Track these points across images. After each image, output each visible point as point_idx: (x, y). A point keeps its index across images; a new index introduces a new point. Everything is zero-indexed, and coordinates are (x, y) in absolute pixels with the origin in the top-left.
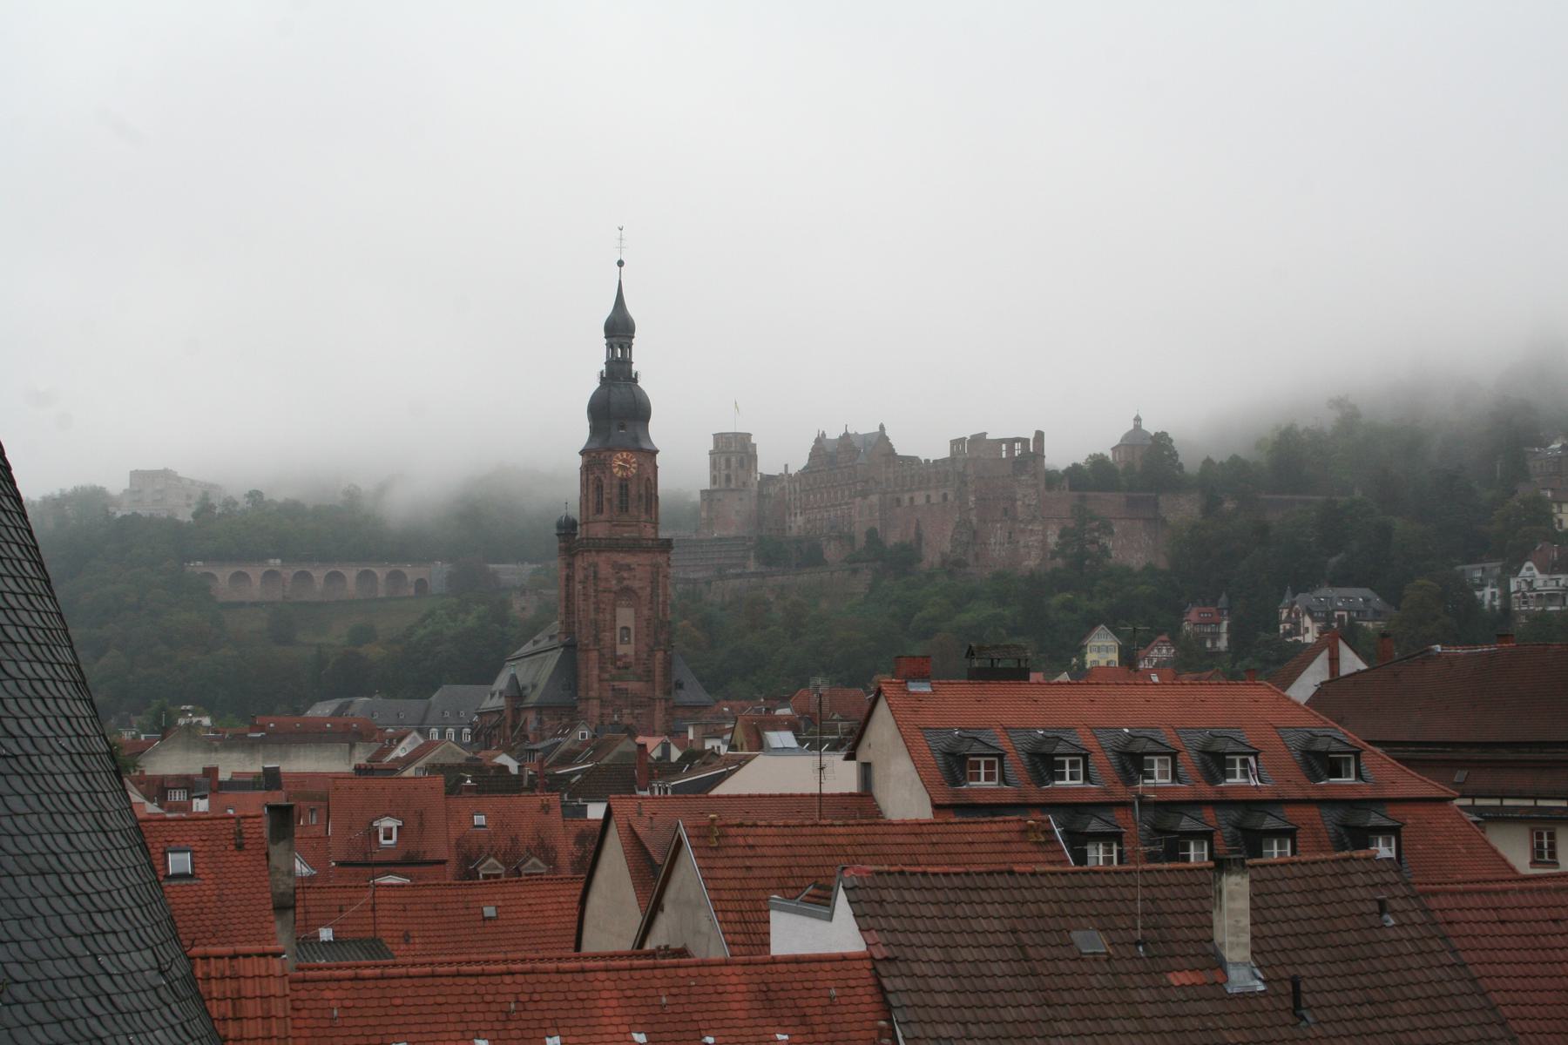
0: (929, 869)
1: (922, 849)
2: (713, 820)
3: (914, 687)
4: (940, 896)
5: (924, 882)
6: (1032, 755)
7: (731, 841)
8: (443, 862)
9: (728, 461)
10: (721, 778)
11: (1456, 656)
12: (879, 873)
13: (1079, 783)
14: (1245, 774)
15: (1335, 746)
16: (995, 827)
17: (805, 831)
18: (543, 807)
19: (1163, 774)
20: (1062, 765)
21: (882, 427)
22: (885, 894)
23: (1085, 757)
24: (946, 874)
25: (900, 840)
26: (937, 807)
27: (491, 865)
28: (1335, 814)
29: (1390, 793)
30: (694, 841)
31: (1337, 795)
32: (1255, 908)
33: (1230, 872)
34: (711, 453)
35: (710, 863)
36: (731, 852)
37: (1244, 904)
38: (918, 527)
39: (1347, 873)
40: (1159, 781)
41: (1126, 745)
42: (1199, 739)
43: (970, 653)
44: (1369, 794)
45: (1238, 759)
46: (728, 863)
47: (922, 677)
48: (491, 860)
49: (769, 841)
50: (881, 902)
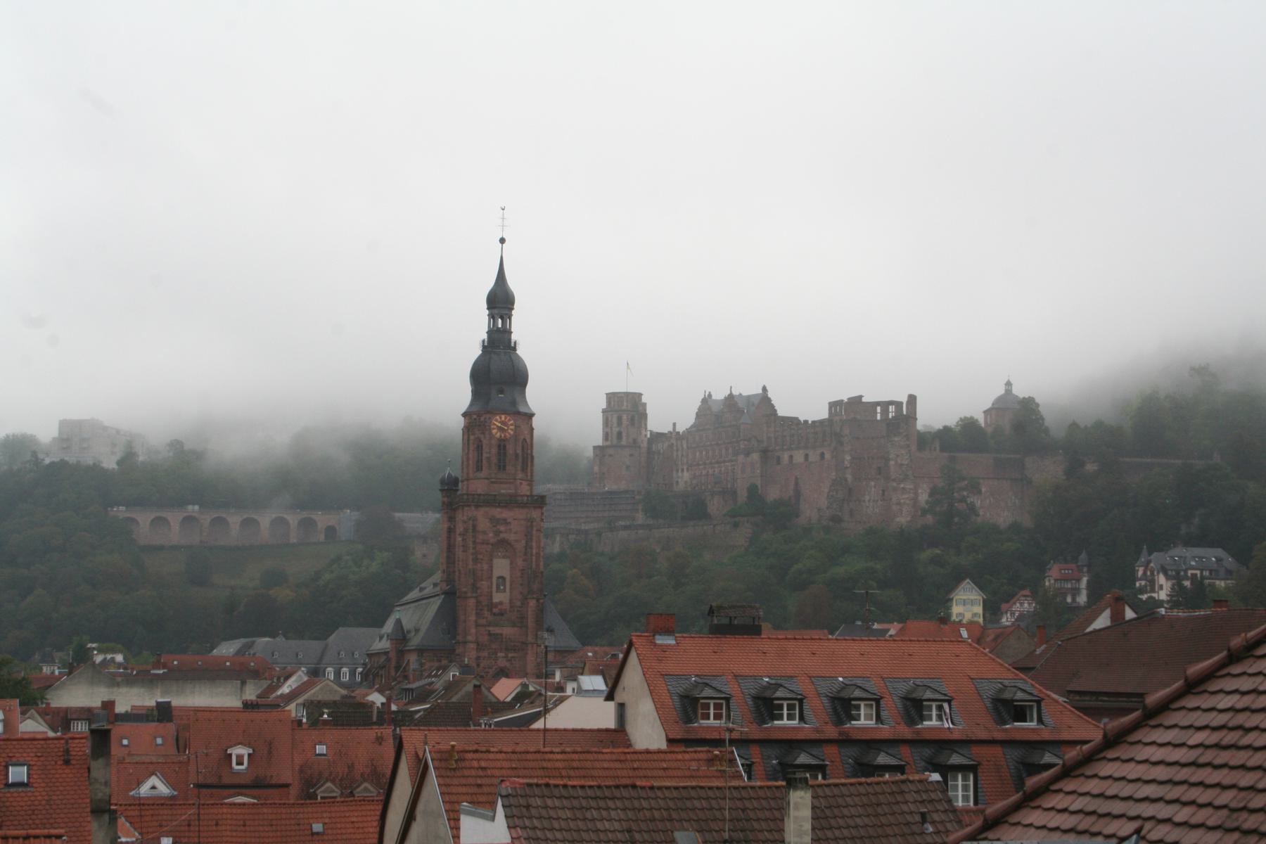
0: (552, 782)
1: (624, 773)
2: (453, 746)
3: (661, 640)
4: (575, 803)
5: (564, 793)
6: (756, 698)
7: (467, 764)
8: (287, 786)
9: (620, 419)
10: (536, 717)
11: (1178, 618)
12: (530, 785)
13: (795, 723)
14: (940, 718)
15: (1020, 695)
16: (687, 756)
17: (530, 757)
18: (377, 738)
19: (868, 717)
20: (780, 707)
21: (764, 389)
22: (532, 801)
23: (801, 701)
24: (582, 787)
25: (606, 765)
26: (670, 741)
27: (328, 789)
28: (1014, 754)
29: (1066, 736)
30: (437, 763)
31: (1018, 737)
32: (815, 818)
33: (796, 788)
34: (604, 411)
35: (448, 781)
36: (466, 773)
37: (807, 813)
38: (797, 484)
39: (902, 792)
40: (863, 722)
41: (839, 692)
42: (903, 688)
43: (711, 612)
44: (1046, 736)
45: (934, 705)
46: (463, 781)
47: (668, 631)
48: (329, 784)
49: (499, 764)
50: (528, 807)
